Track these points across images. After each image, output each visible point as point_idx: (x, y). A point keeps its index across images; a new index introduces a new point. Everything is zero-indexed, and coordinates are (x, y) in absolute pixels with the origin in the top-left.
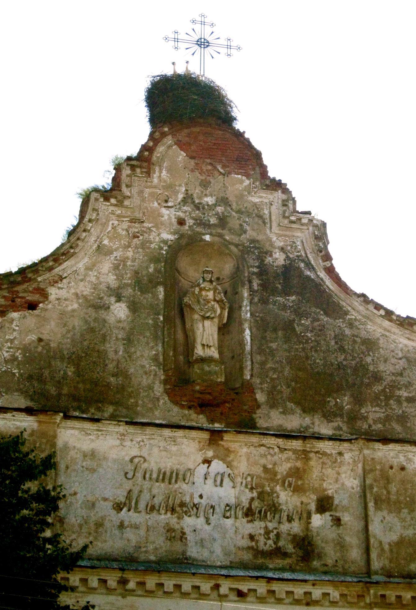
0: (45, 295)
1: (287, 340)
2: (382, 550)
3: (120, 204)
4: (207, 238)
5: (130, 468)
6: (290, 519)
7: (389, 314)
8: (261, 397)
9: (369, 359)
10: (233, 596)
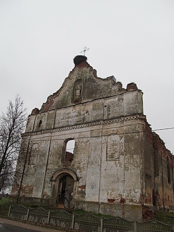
0: (59, 94)
1: (87, 89)
2: (93, 117)
3: (69, 78)
4: (79, 78)
5: (64, 114)
6: (82, 116)
7: (102, 79)
8: (82, 99)
9: (98, 88)
10: (72, 129)
